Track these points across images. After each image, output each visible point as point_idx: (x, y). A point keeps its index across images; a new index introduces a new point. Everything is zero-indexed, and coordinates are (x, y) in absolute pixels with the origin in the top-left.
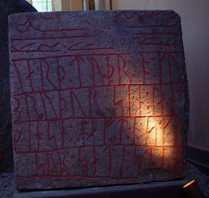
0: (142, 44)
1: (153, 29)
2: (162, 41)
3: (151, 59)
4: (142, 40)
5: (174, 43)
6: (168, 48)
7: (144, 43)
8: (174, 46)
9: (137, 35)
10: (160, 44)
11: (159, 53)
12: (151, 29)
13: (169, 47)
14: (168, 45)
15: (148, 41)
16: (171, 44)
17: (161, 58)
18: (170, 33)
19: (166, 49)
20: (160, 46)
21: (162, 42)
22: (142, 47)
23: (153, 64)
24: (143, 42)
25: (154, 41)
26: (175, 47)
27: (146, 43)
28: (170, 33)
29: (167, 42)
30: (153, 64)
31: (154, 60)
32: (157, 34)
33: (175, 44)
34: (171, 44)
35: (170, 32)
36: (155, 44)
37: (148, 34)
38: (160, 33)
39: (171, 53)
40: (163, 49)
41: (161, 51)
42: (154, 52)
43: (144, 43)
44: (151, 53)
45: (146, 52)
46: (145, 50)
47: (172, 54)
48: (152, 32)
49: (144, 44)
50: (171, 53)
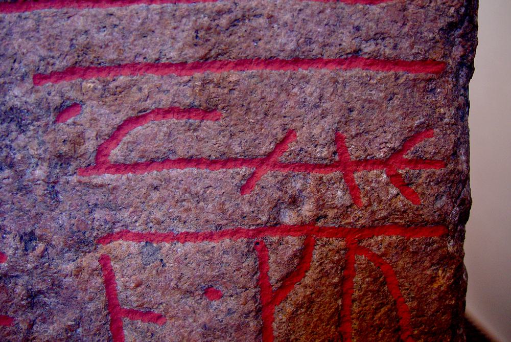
0: (100, 161)
1: (205, 21)
2: (290, 134)
3: (189, 293)
4: (91, 133)
5: (396, 153)
6: (340, 196)
7: (116, 153)
8: (395, 179)
9: (40, 78)
10: (266, 160)
11: (259, 237)
12: (188, 25)
13: (353, 190)
14: (342, 163)
15: (149, 136)
16: (370, 163)
17: (275, 274)
18: (375, 62)
19: (321, 205)
20: (268, 178)
21: (292, 146)
22: (95, 197)
23: (205, 326)
24: (101, 151)
25: (210, 137)
26: (403, 185)
27: (134, 157)
28: (375, 62)
29: (338, 140)
30: (205, 326)
31: (210, 292)
32: (242, 63)
33: (408, 156)
34: (370, 163)
35: (369, 48)
36: (226, 161)
37: (156, 66)
38: (270, 62)
39: (373, 229)
40: (294, 202)
41: (275, 226)
42: (210, 237)
43: (116, 153)
44: (185, 237)
45: (139, 237)
46: (125, 215)
47: (379, 242)
48: (192, 54)
49: (119, 167)
50: (373, 229)
